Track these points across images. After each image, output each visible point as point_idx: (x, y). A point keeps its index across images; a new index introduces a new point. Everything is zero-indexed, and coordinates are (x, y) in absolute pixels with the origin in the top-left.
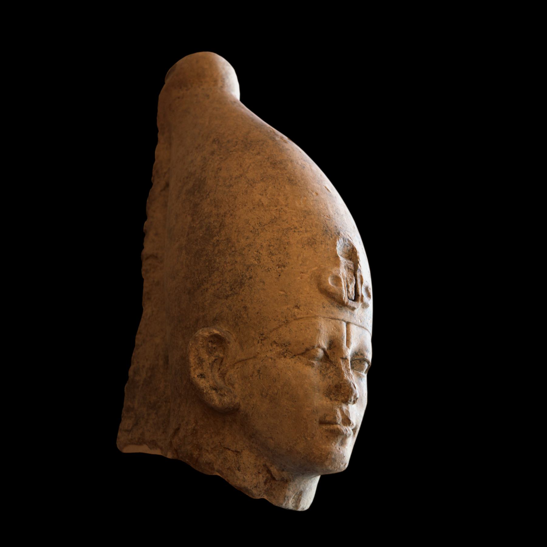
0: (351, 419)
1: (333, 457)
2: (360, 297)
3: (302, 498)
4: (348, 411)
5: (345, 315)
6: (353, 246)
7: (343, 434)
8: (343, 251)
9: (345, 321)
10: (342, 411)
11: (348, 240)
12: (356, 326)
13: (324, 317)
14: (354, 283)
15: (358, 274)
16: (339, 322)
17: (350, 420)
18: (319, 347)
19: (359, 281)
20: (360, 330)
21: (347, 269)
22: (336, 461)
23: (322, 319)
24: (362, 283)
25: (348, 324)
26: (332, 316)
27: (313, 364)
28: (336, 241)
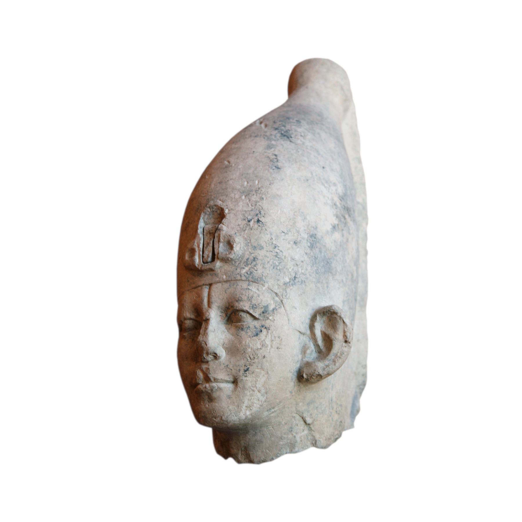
0: (210, 376)
1: (203, 415)
2: (216, 257)
3: (251, 453)
4: (208, 369)
5: (207, 279)
6: (221, 208)
7: (202, 392)
8: (215, 218)
9: (206, 285)
10: (202, 371)
11: (215, 205)
12: (220, 284)
13: (188, 290)
14: (211, 245)
15: (216, 235)
16: (200, 288)
17: (208, 377)
18: (185, 319)
19: (216, 240)
20: (226, 285)
21: (208, 235)
22: (207, 418)
23: (187, 292)
24: (219, 241)
25: (210, 285)
26: (194, 286)
27: (184, 336)
28: (200, 214)
